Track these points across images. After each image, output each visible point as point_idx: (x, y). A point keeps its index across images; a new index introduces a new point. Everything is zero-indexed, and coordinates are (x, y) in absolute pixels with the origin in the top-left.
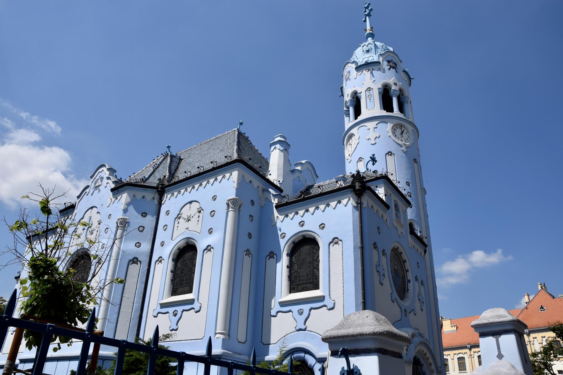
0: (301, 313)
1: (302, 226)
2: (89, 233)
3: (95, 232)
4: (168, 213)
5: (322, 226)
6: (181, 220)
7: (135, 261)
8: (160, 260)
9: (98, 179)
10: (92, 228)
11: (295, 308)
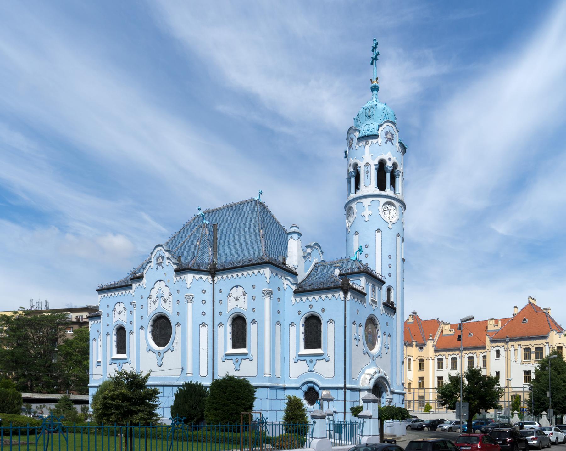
0: (311, 361)
1: (311, 308)
2: (163, 302)
3: (168, 301)
4: (221, 291)
5: (323, 310)
6: (231, 298)
10: (165, 297)
11: (308, 359)
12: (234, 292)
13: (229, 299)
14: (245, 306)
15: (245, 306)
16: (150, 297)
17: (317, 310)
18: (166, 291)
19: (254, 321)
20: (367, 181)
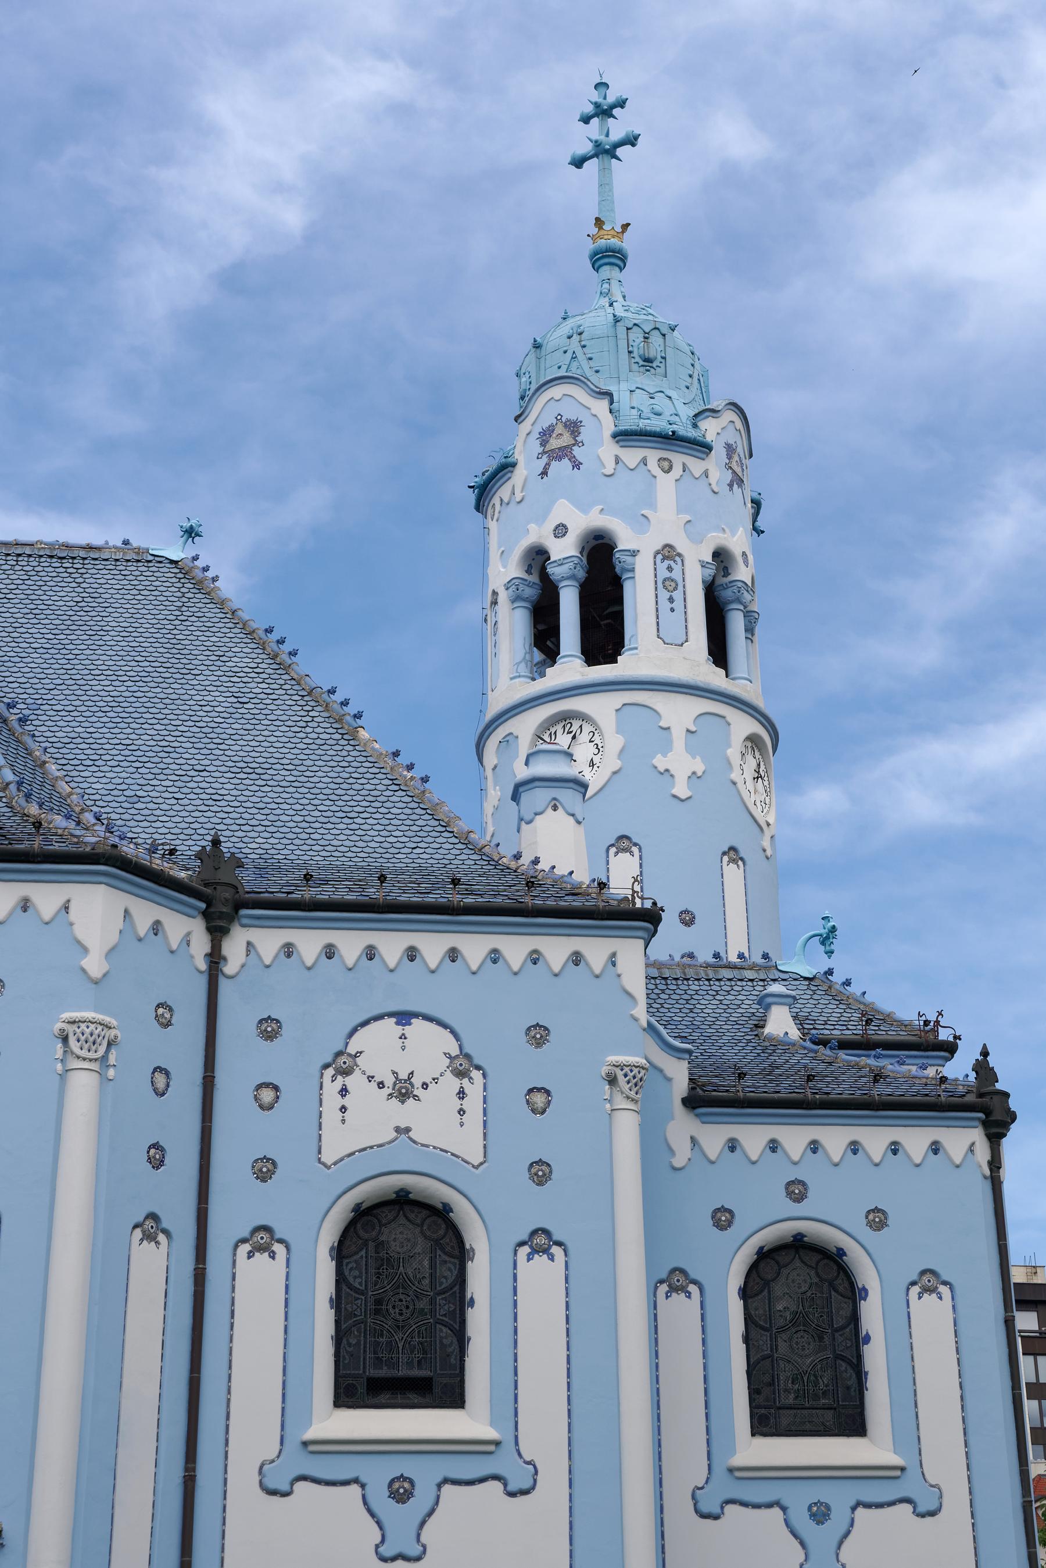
4: (269, 1029)
5: (877, 1219)
6: (354, 1081)
7: (151, 1227)
8: (263, 1239)
12: (379, 1047)
13: (331, 1089)
14: (469, 1143)
15: (469, 1143)
17: (831, 1214)
19: (540, 1241)
20: (672, 623)
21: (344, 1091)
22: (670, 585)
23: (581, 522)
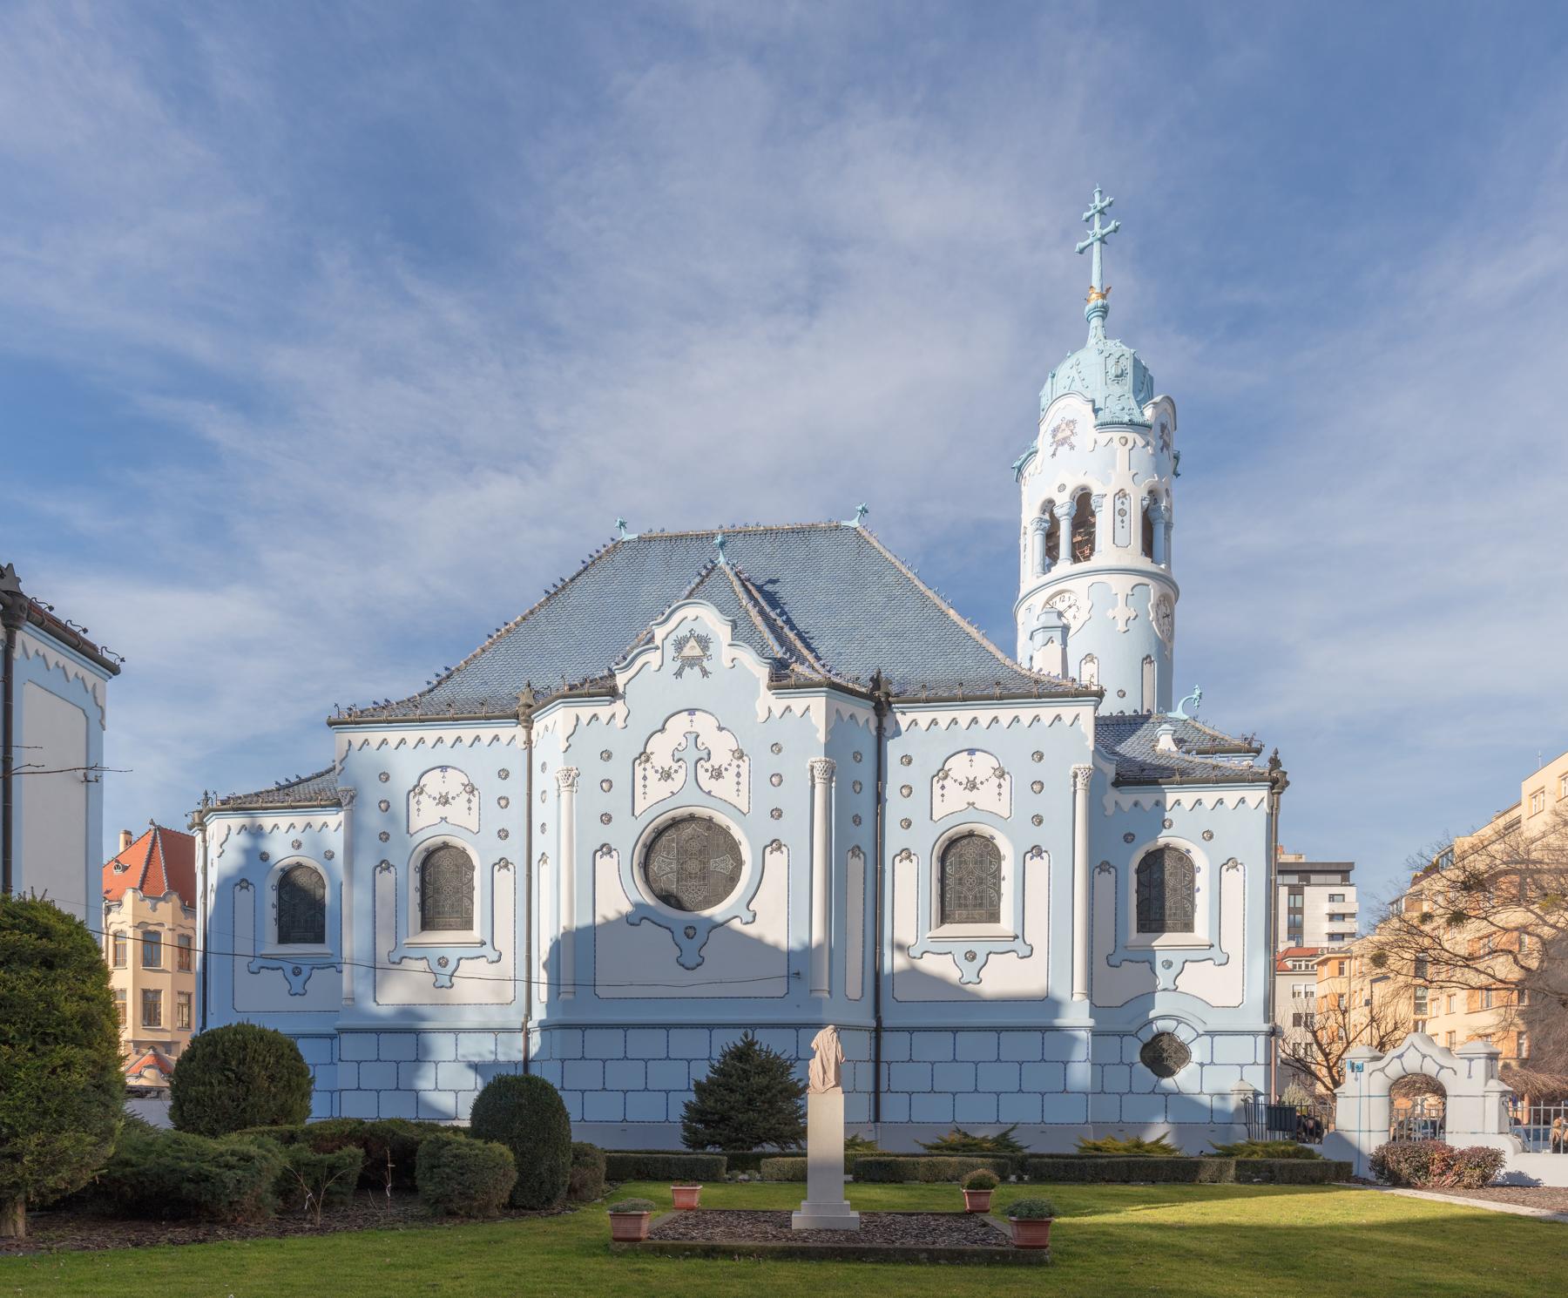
3: (730, 776)
6: (947, 783)
7: (856, 850)
8: (906, 854)
9: (685, 640)
12: (960, 767)
16: (644, 756)
18: (721, 748)
21: (943, 787)
22: (1122, 513)
23: (1072, 484)
